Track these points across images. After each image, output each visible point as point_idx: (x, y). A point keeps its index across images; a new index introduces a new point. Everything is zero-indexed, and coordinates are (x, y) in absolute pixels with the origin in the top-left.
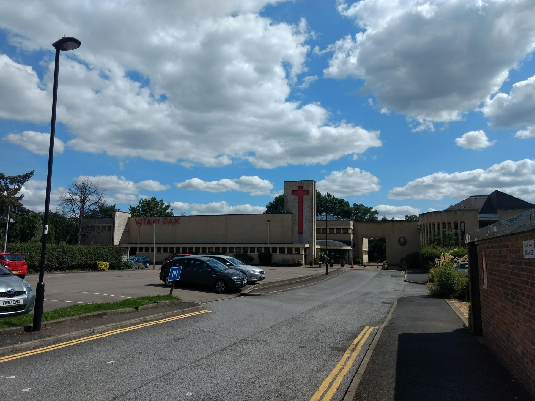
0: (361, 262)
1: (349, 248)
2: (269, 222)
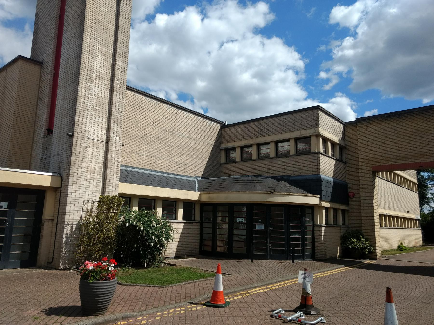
0: (370, 252)
1: (314, 200)
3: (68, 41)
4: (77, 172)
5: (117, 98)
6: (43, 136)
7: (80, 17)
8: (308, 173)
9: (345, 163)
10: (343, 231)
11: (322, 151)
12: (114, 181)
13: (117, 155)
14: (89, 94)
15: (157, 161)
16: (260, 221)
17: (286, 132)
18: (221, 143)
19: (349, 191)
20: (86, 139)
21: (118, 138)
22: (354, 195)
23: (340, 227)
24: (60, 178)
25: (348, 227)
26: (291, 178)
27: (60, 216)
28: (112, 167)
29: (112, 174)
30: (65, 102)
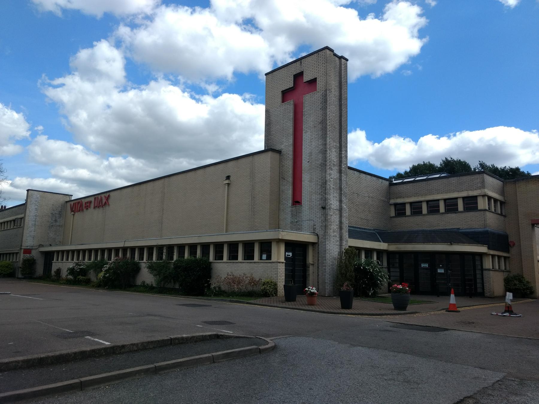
2: (227, 182)
3: (310, 139)
4: (329, 232)
5: (344, 178)
6: (290, 206)
7: (321, 124)
8: (476, 226)
9: (505, 216)
10: (506, 275)
11: (487, 209)
12: (346, 237)
13: (346, 219)
14: (331, 178)
15: (349, 218)
16: (441, 266)
17: (454, 191)
18: (390, 199)
19: (509, 240)
20: (331, 210)
21: (346, 207)
22: (514, 244)
23: (503, 271)
24: (316, 237)
25: (509, 272)
26: (460, 231)
27: (320, 262)
28: (344, 227)
29: (344, 233)
30: (312, 183)
